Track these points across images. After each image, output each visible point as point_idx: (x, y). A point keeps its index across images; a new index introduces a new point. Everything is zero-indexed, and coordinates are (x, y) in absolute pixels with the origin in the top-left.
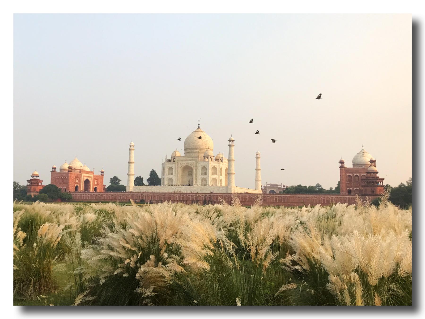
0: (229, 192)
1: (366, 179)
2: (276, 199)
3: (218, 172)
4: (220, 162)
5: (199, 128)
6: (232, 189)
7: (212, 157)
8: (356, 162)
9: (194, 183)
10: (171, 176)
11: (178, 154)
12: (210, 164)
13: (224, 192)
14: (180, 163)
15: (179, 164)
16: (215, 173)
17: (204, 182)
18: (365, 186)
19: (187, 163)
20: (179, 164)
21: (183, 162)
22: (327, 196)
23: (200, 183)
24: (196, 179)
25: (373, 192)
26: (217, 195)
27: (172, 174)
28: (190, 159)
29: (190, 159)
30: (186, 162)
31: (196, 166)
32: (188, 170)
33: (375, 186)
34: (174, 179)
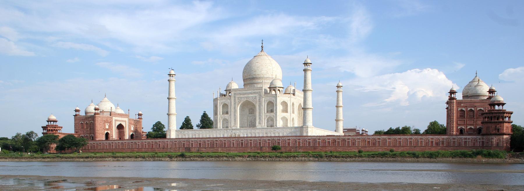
0: (305, 134)
1: (489, 113)
2: (369, 142)
3: (289, 109)
4: (292, 96)
6: (309, 129)
7: (281, 89)
8: (470, 93)
10: (226, 116)
11: (235, 86)
12: (278, 98)
13: (298, 134)
16: (285, 110)
17: (270, 123)
18: (487, 123)
19: (247, 97)
21: (241, 96)
22: (436, 137)
23: (264, 124)
25: (498, 130)
26: (288, 138)
27: (227, 113)
28: (250, 91)
29: (250, 91)
30: (246, 96)
31: (260, 101)
32: (249, 108)
33: (501, 122)
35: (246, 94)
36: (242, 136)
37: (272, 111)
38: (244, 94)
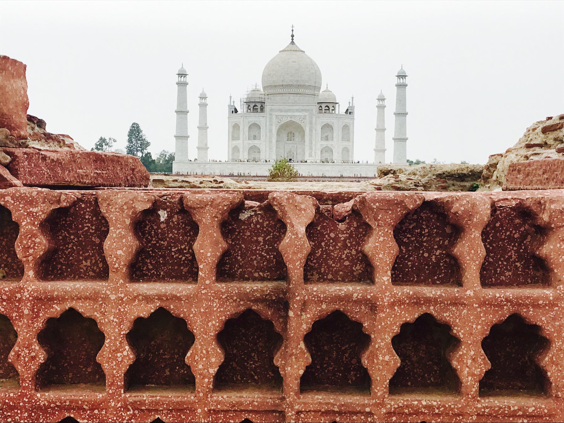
10: (256, 142)
14: (277, 116)
15: (274, 117)
20: (274, 117)
24: (311, 148)
27: (255, 138)
30: (289, 114)
31: (311, 123)
34: (262, 148)
37: (327, 139)
38: (286, 111)
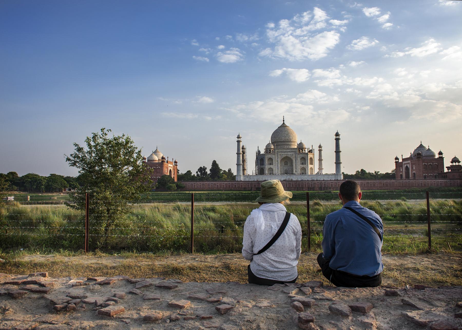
5: (284, 123)
9: (294, 172)
10: (271, 166)
24: (296, 168)
27: (270, 164)
31: (296, 157)
34: (274, 169)
35: (285, 152)
36: (294, 179)
37: (303, 164)
